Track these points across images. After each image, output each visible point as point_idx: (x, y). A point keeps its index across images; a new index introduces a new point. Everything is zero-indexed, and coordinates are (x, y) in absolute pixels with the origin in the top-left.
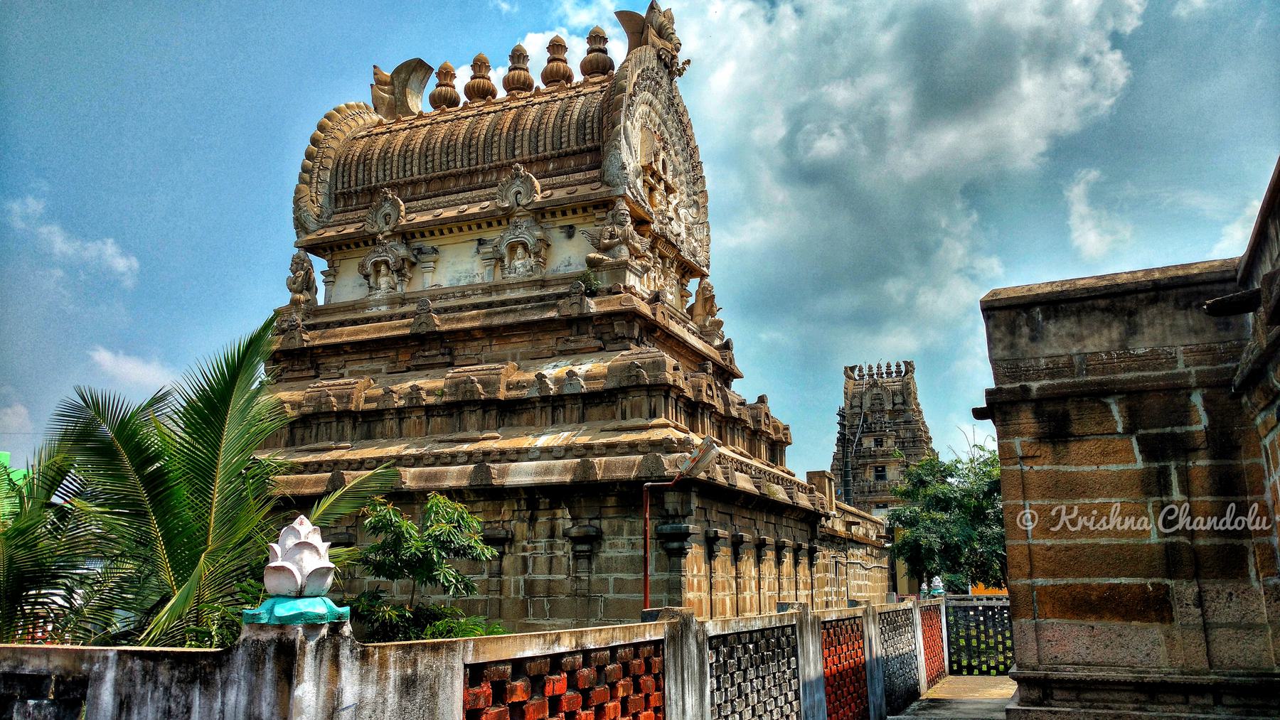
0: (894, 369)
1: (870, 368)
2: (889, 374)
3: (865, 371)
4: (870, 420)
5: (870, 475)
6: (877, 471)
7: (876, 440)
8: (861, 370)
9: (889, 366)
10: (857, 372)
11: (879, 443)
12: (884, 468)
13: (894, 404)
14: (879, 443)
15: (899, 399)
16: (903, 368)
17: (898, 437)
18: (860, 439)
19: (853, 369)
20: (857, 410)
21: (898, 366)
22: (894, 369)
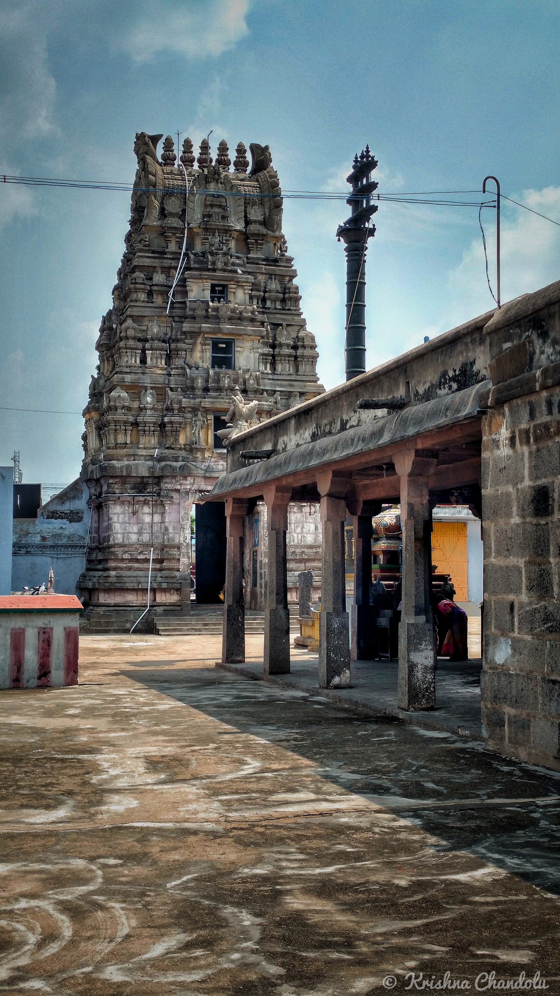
0: (232, 155)
1: (188, 145)
2: (223, 162)
3: (178, 151)
4: (198, 248)
5: (201, 356)
6: (215, 349)
7: (213, 291)
8: (169, 145)
9: (223, 148)
10: (160, 151)
11: (219, 292)
12: (230, 344)
13: (248, 222)
14: (219, 292)
15: (256, 214)
16: (249, 156)
17: (255, 286)
18: (183, 282)
19: (155, 139)
20: (174, 222)
21: (241, 150)
22: (232, 155)
